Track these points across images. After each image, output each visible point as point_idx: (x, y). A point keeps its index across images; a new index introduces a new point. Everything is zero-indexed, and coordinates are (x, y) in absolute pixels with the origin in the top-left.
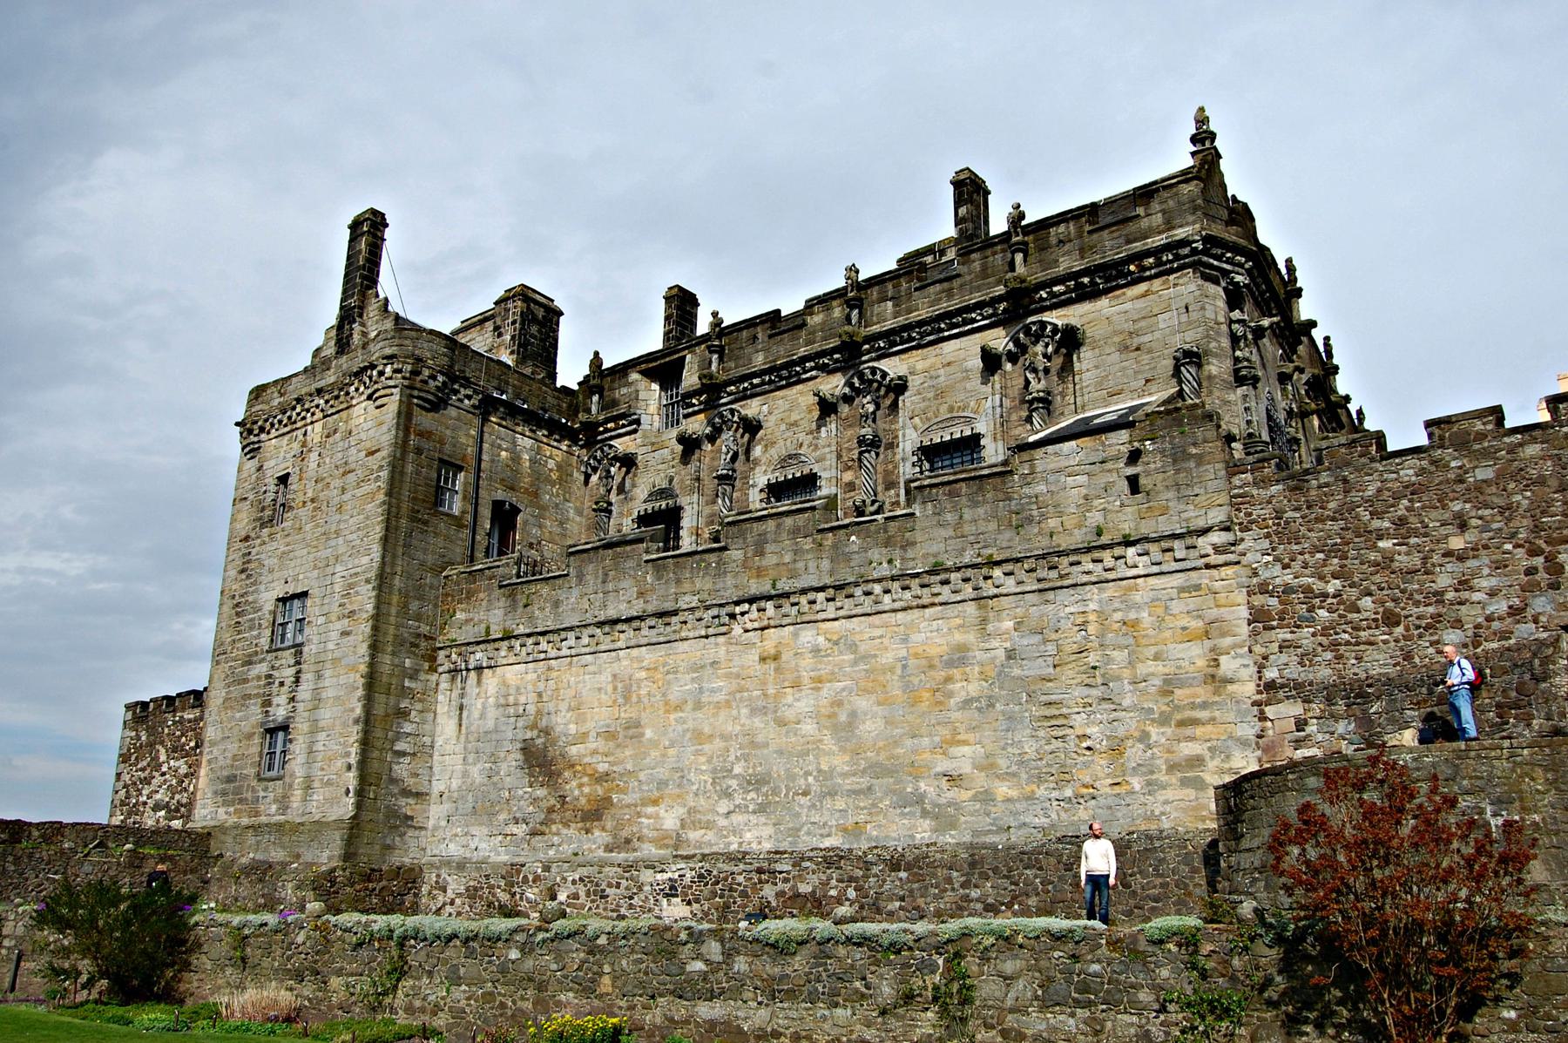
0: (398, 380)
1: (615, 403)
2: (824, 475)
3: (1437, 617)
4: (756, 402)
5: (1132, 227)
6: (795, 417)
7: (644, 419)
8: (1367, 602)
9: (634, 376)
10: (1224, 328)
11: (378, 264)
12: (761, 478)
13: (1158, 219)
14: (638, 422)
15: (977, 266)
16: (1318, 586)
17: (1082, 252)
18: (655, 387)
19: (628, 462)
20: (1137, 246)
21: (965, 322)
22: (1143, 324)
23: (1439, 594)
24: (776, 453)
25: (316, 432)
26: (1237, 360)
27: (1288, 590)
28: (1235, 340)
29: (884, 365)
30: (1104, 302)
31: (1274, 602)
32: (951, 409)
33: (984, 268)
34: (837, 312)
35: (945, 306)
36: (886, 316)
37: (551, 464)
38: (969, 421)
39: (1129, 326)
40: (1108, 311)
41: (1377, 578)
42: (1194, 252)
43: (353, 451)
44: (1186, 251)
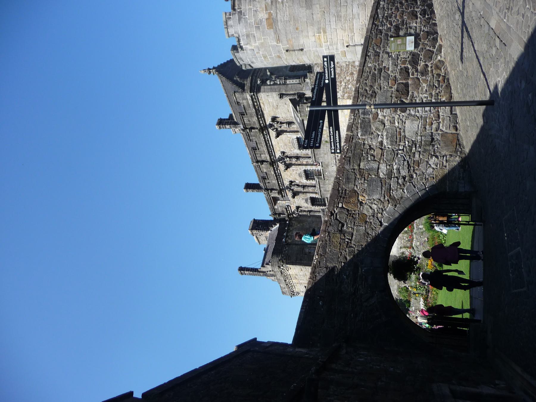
0: (284, 265)
1: (283, 211)
2: (304, 168)
3: (352, 66)
4: (284, 182)
5: (246, 106)
6: (289, 174)
7: (287, 204)
8: (347, 78)
9: (276, 207)
10: (272, 87)
11: (252, 268)
12: (304, 181)
13: (244, 101)
14: (288, 206)
15: (253, 138)
16: (343, 87)
17: (252, 116)
18: (278, 202)
19: (298, 208)
20: (251, 106)
21: (268, 141)
22: (271, 105)
23: (347, 65)
24: (298, 178)
25: (295, 281)
26: (280, 84)
27: (343, 92)
28: (275, 84)
29: (277, 156)
30: (265, 112)
31: (346, 95)
32: (290, 143)
33: (254, 136)
34: (263, 166)
35: (264, 144)
36: (266, 156)
37: (298, 225)
38: (293, 139)
39: (271, 108)
40: (267, 112)
41: (342, 76)
42: (254, 95)
43: (301, 274)
44: (253, 97)
